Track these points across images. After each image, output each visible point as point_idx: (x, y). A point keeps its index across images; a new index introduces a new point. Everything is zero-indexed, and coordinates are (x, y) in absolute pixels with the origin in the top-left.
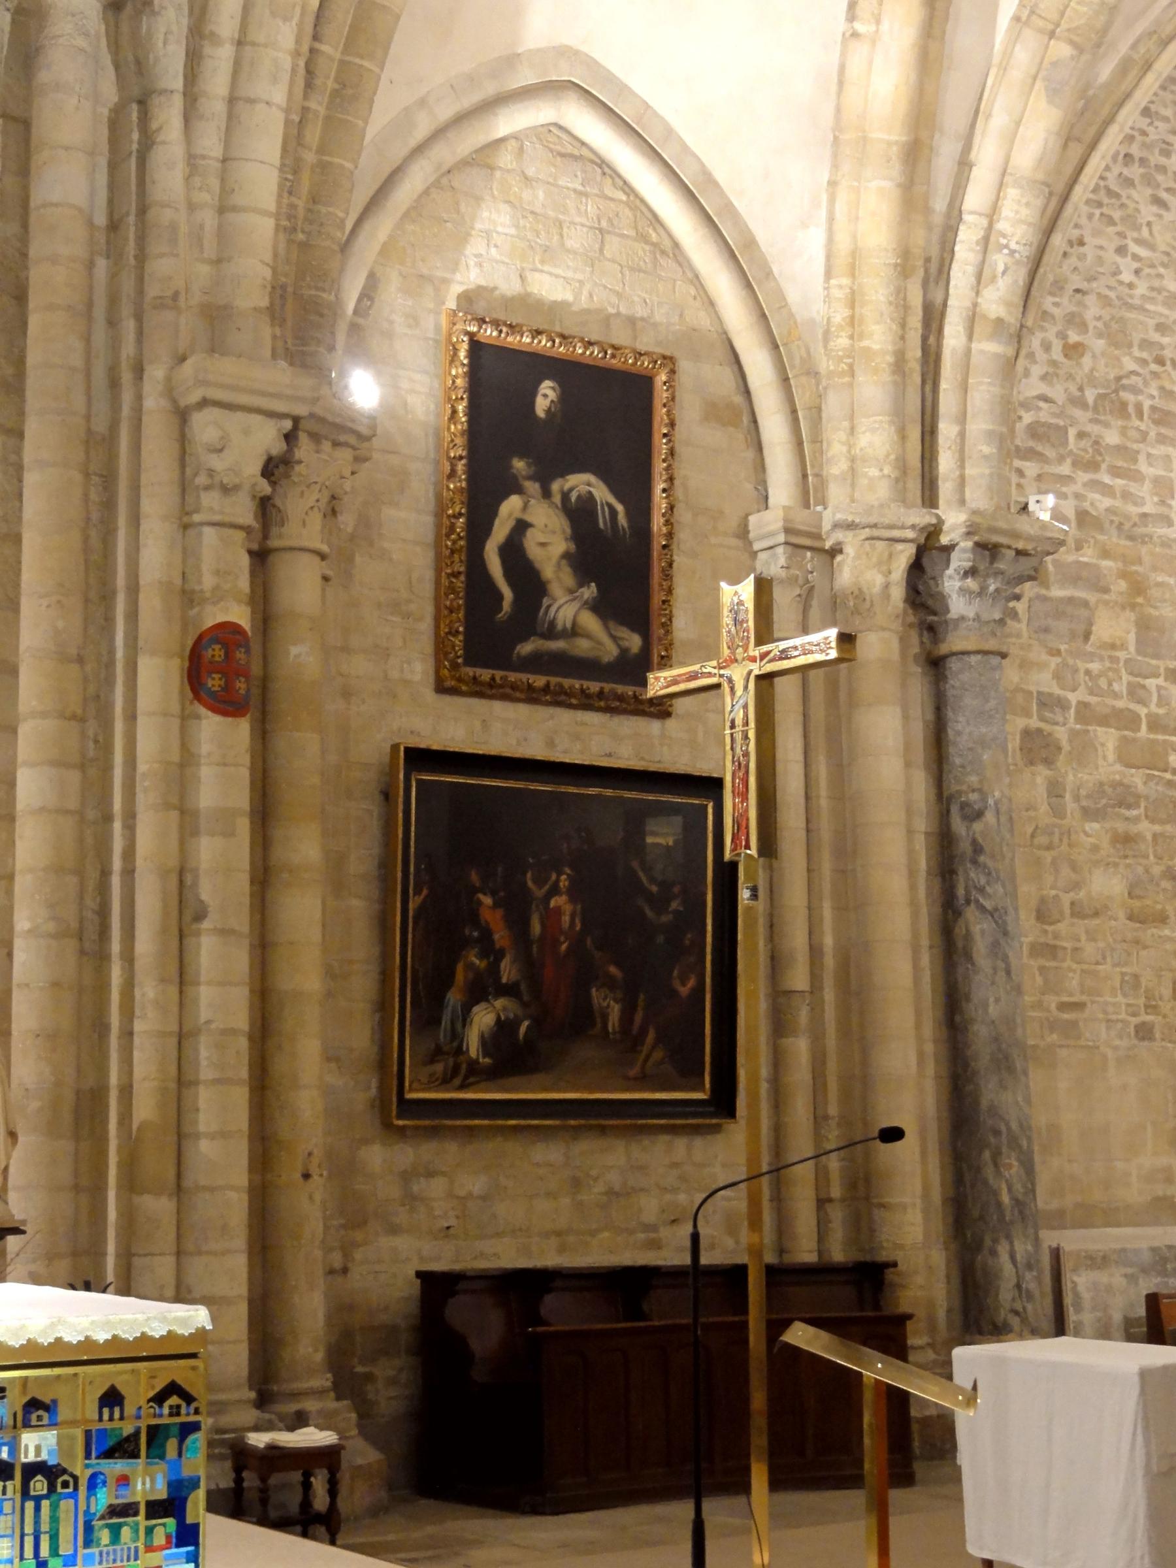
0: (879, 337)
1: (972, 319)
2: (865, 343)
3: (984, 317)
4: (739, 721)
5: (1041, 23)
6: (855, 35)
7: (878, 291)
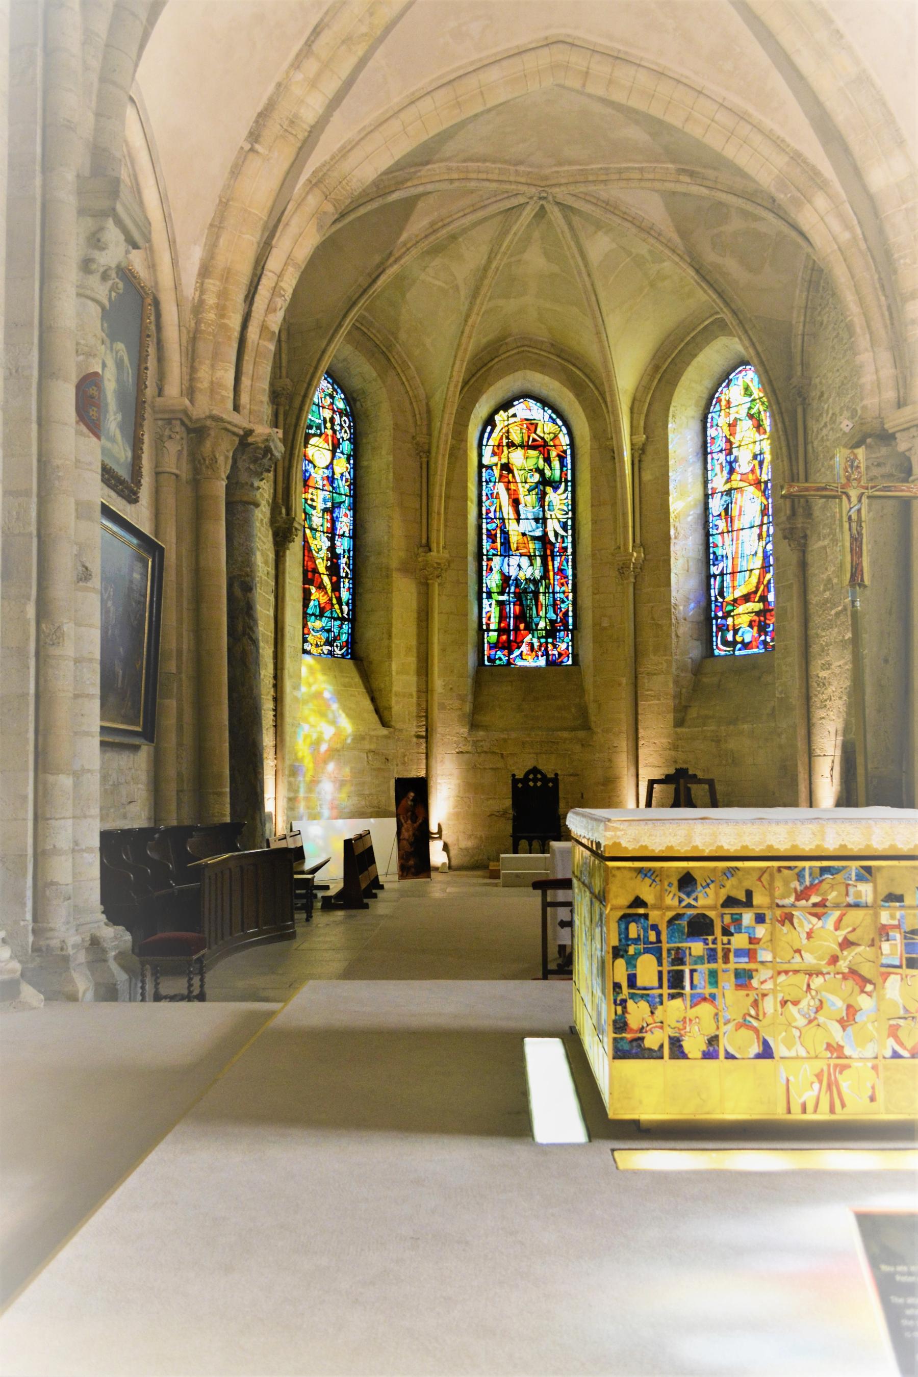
0: (235, 322)
1: (264, 328)
2: (226, 321)
3: (267, 328)
4: (854, 517)
5: (325, 190)
6: (252, 150)
7: (238, 296)
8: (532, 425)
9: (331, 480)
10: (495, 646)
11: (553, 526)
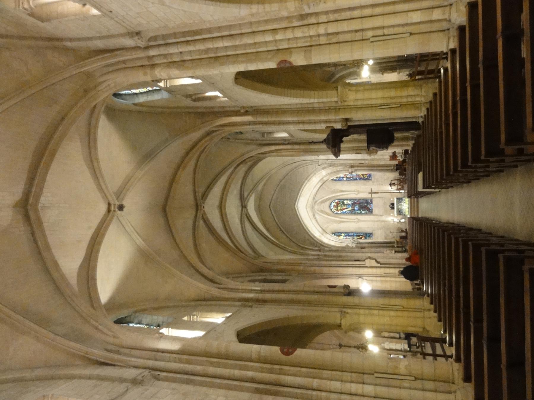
8: (334, 206)
9: (345, 236)
10: (369, 212)
11: (350, 203)
